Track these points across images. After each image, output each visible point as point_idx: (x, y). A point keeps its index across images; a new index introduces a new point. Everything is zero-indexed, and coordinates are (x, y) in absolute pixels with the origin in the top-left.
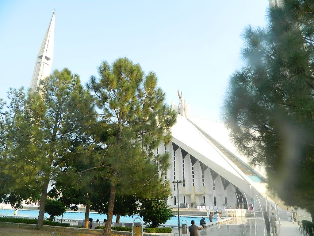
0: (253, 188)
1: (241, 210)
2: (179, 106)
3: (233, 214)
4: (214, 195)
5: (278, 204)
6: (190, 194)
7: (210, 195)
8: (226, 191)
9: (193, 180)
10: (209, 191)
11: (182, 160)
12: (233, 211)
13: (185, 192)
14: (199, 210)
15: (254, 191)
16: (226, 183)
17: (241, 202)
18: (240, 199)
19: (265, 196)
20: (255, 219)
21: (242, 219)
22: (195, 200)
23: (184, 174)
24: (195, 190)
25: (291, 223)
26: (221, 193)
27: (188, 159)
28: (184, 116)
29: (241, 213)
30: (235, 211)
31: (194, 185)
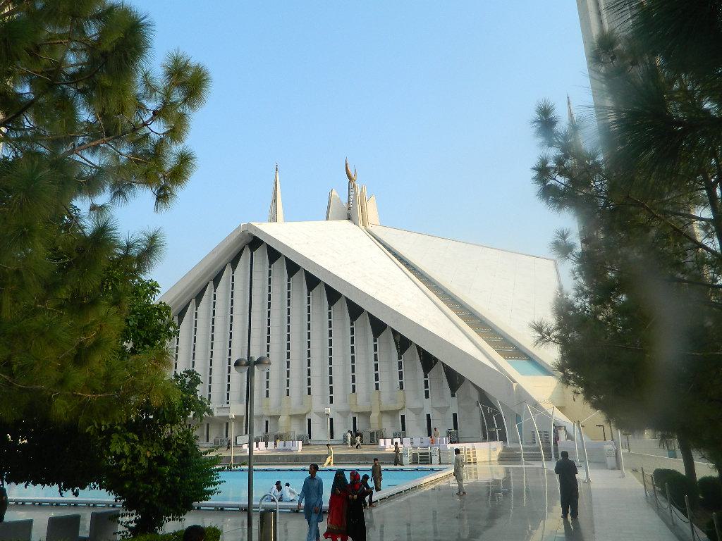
0: (519, 387)
2: (349, 202)
3: (469, 453)
4: (427, 411)
5: (583, 426)
7: (417, 411)
8: (455, 399)
9: (377, 376)
10: (415, 401)
11: (349, 327)
12: (468, 449)
14: (384, 448)
15: (523, 397)
16: (455, 380)
17: (491, 425)
18: (489, 417)
19: (548, 407)
20: (524, 466)
21: (491, 468)
22: (380, 423)
23: (353, 362)
24: (379, 401)
25: (617, 473)
26: (443, 404)
27: (363, 324)
28: (361, 225)
29: (490, 452)
30: (474, 449)
31: (377, 389)
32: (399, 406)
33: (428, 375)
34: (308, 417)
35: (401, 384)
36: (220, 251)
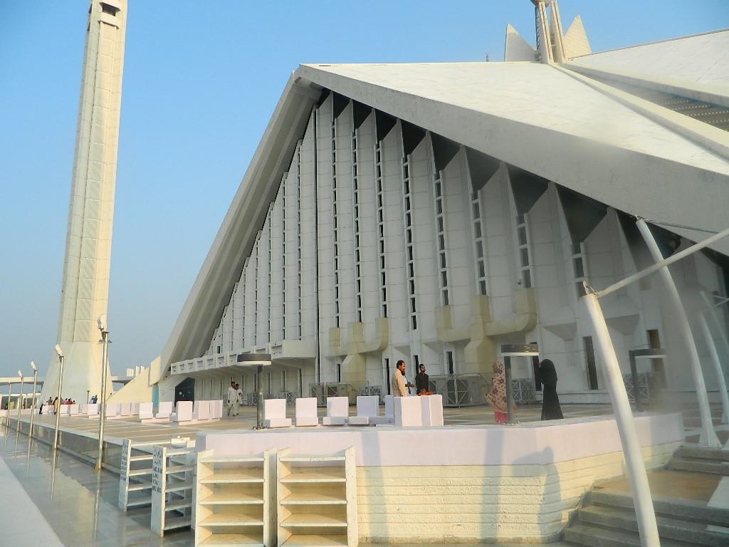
1: (494, 447)
6: (465, 337)
13: (448, 326)
24: (485, 315)
28: (551, 61)
29: (491, 487)
32: (520, 323)
33: (582, 245)
34: (384, 357)
35: (526, 273)
36: (277, 117)
